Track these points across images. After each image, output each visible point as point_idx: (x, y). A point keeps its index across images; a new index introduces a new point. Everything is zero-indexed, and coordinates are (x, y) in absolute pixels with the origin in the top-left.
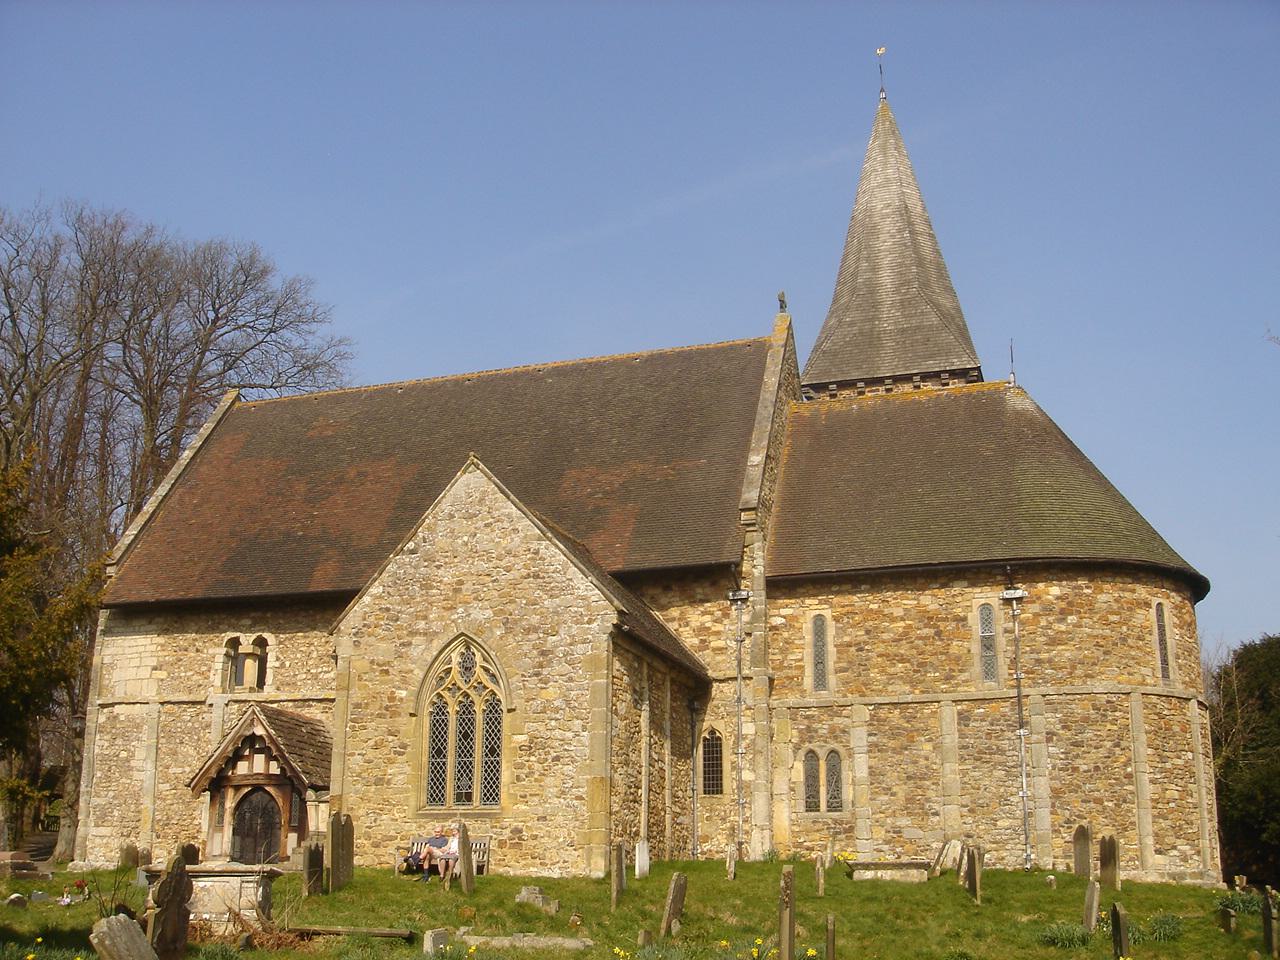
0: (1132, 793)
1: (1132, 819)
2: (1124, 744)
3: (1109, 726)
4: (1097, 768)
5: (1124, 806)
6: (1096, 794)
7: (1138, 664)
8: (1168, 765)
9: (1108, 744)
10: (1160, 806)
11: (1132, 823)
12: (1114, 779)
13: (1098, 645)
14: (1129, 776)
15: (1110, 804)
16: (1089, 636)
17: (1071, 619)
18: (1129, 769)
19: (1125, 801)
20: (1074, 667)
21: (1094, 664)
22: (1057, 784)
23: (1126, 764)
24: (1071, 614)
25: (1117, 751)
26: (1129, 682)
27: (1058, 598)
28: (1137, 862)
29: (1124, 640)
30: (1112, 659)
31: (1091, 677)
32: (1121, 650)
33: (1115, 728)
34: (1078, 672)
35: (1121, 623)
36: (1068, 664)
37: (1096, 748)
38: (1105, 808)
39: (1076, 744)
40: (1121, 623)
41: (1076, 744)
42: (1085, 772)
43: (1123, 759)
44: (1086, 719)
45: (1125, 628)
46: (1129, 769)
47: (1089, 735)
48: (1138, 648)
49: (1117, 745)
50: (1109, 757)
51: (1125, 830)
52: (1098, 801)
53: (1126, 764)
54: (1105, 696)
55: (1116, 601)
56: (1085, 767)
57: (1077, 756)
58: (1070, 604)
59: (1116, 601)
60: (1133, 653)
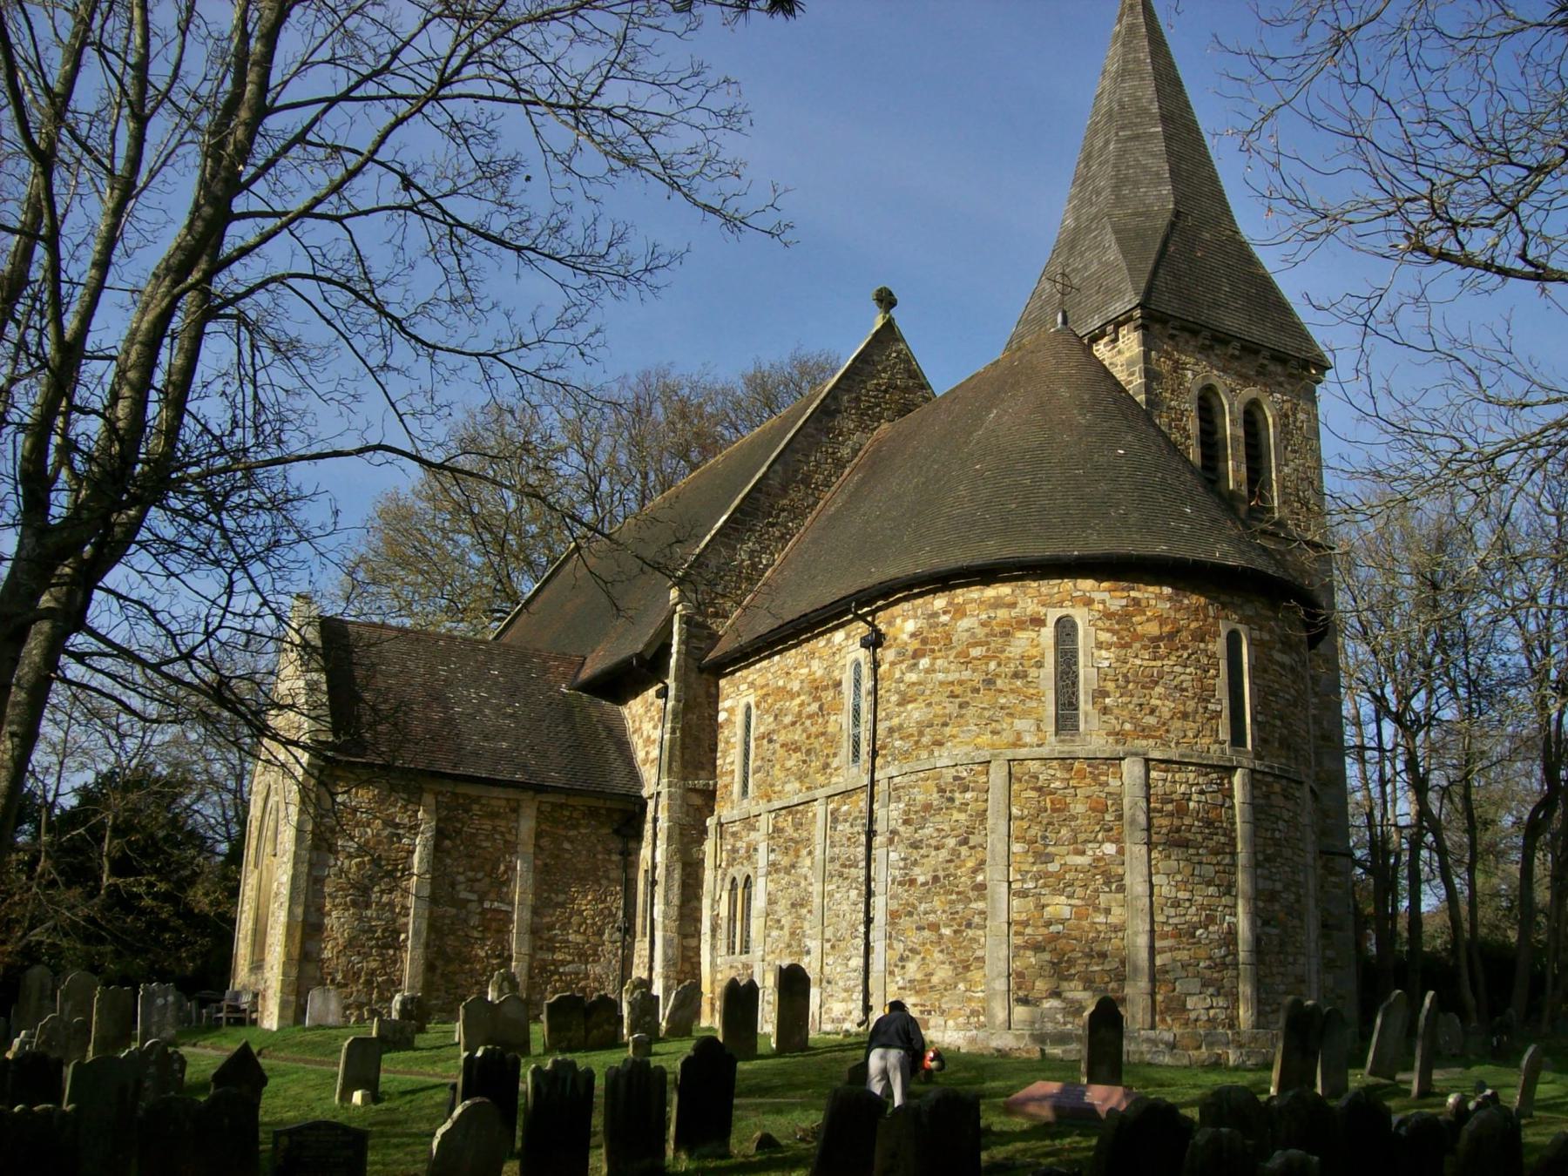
0: (982, 913)
1: (979, 953)
2: (973, 840)
3: (956, 815)
4: (936, 879)
5: (970, 933)
6: (932, 918)
7: (1011, 715)
8: (1053, 867)
9: (951, 842)
10: (1029, 930)
11: (977, 959)
12: (958, 893)
13: (953, 695)
14: (981, 888)
15: (946, 931)
16: (941, 683)
17: (924, 663)
18: (980, 878)
19: (969, 925)
20: (921, 734)
21: (945, 724)
22: (894, 905)
23: (975, 871)
24: (924, 656)
25: (964, 850)
26: (993, 746)
27: (913, 635)
28: (982, 1018)
29: (989, 682)
30: (970, 712)
31: (941, 744)
32: (984, 699)
33: (963, 817)
34: (925, 740)
35: (987, 659)
36: (914, 731)
37: (937, 848)
38: (941, 936)
39: (915, 846)
40: (987, 659)
41: (915, 846)
42: (923, 884)
43: (970, 864)
44: (927, 807)
45: (993, 665)
46: (980, 878)
47: (929, 831)
48: (1012, 691)
49: (965, 842)
50: (951, 861)
51: (967, 968)
52: (934, 927)
53: (975, 871)
54: (953, 770)
55: (983, 625)
56: (921, 879)
57: (915, 863)
58: (924, 642)
59: (983, 625)
60: (1003, 701)
